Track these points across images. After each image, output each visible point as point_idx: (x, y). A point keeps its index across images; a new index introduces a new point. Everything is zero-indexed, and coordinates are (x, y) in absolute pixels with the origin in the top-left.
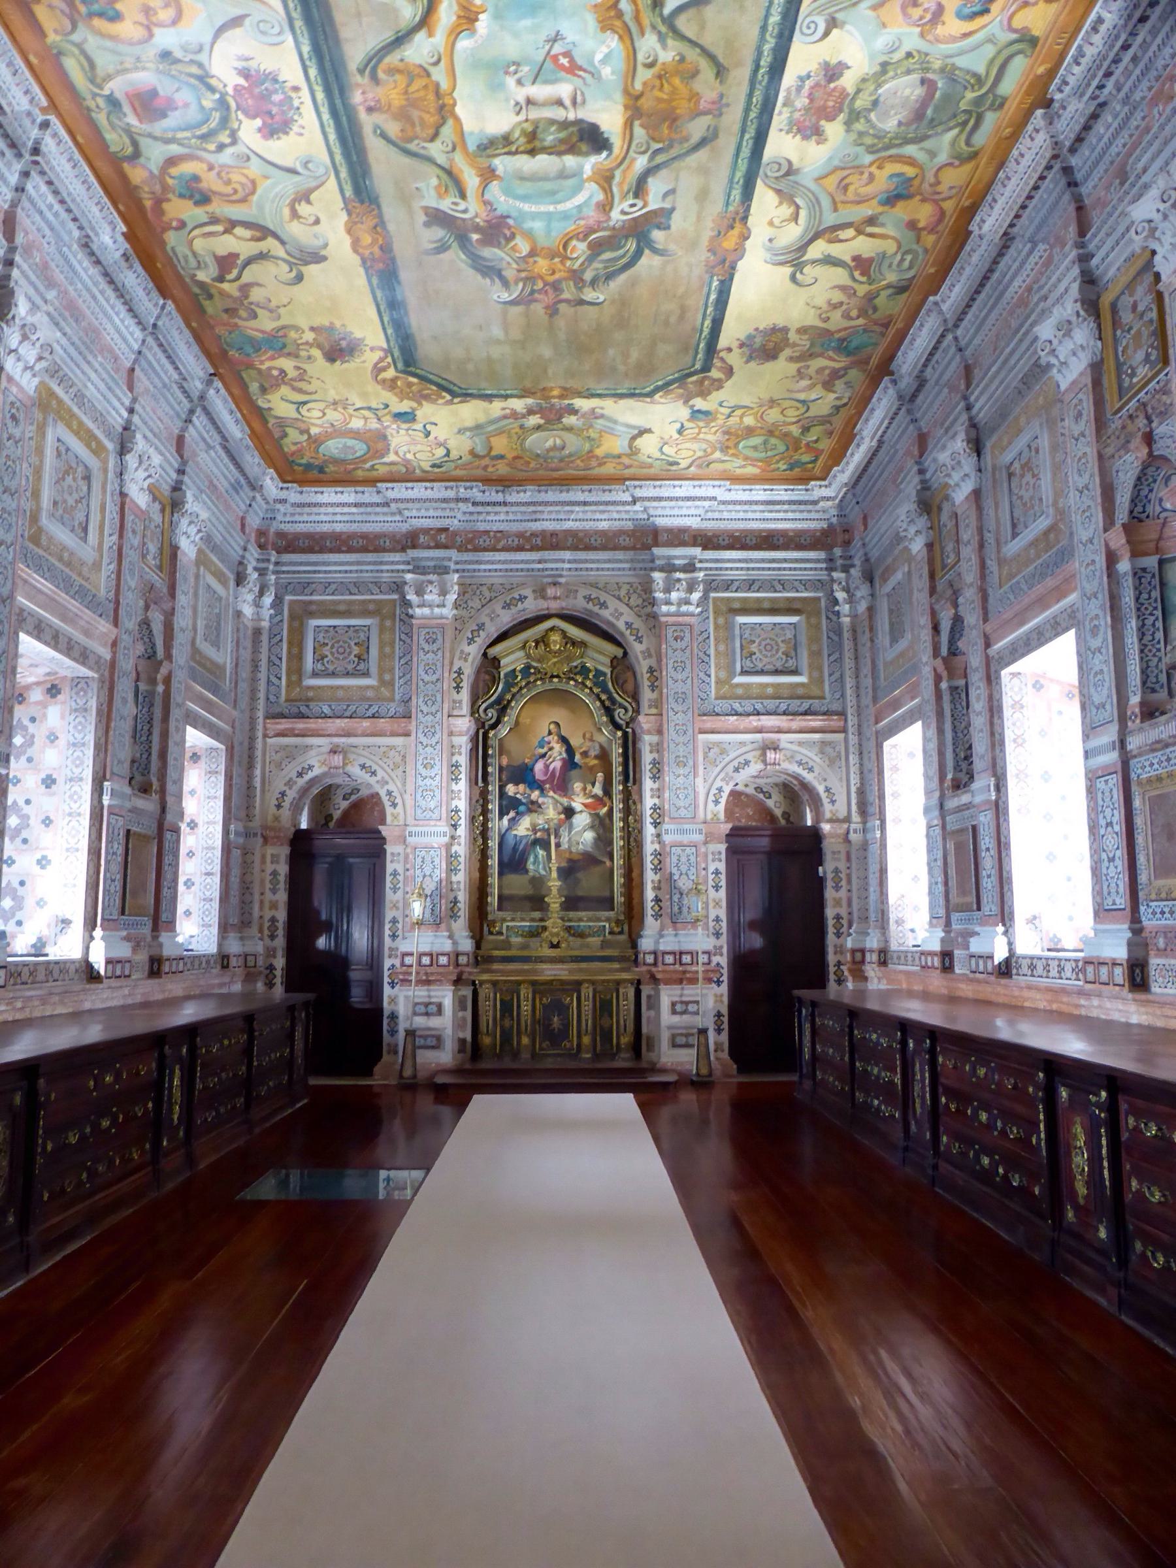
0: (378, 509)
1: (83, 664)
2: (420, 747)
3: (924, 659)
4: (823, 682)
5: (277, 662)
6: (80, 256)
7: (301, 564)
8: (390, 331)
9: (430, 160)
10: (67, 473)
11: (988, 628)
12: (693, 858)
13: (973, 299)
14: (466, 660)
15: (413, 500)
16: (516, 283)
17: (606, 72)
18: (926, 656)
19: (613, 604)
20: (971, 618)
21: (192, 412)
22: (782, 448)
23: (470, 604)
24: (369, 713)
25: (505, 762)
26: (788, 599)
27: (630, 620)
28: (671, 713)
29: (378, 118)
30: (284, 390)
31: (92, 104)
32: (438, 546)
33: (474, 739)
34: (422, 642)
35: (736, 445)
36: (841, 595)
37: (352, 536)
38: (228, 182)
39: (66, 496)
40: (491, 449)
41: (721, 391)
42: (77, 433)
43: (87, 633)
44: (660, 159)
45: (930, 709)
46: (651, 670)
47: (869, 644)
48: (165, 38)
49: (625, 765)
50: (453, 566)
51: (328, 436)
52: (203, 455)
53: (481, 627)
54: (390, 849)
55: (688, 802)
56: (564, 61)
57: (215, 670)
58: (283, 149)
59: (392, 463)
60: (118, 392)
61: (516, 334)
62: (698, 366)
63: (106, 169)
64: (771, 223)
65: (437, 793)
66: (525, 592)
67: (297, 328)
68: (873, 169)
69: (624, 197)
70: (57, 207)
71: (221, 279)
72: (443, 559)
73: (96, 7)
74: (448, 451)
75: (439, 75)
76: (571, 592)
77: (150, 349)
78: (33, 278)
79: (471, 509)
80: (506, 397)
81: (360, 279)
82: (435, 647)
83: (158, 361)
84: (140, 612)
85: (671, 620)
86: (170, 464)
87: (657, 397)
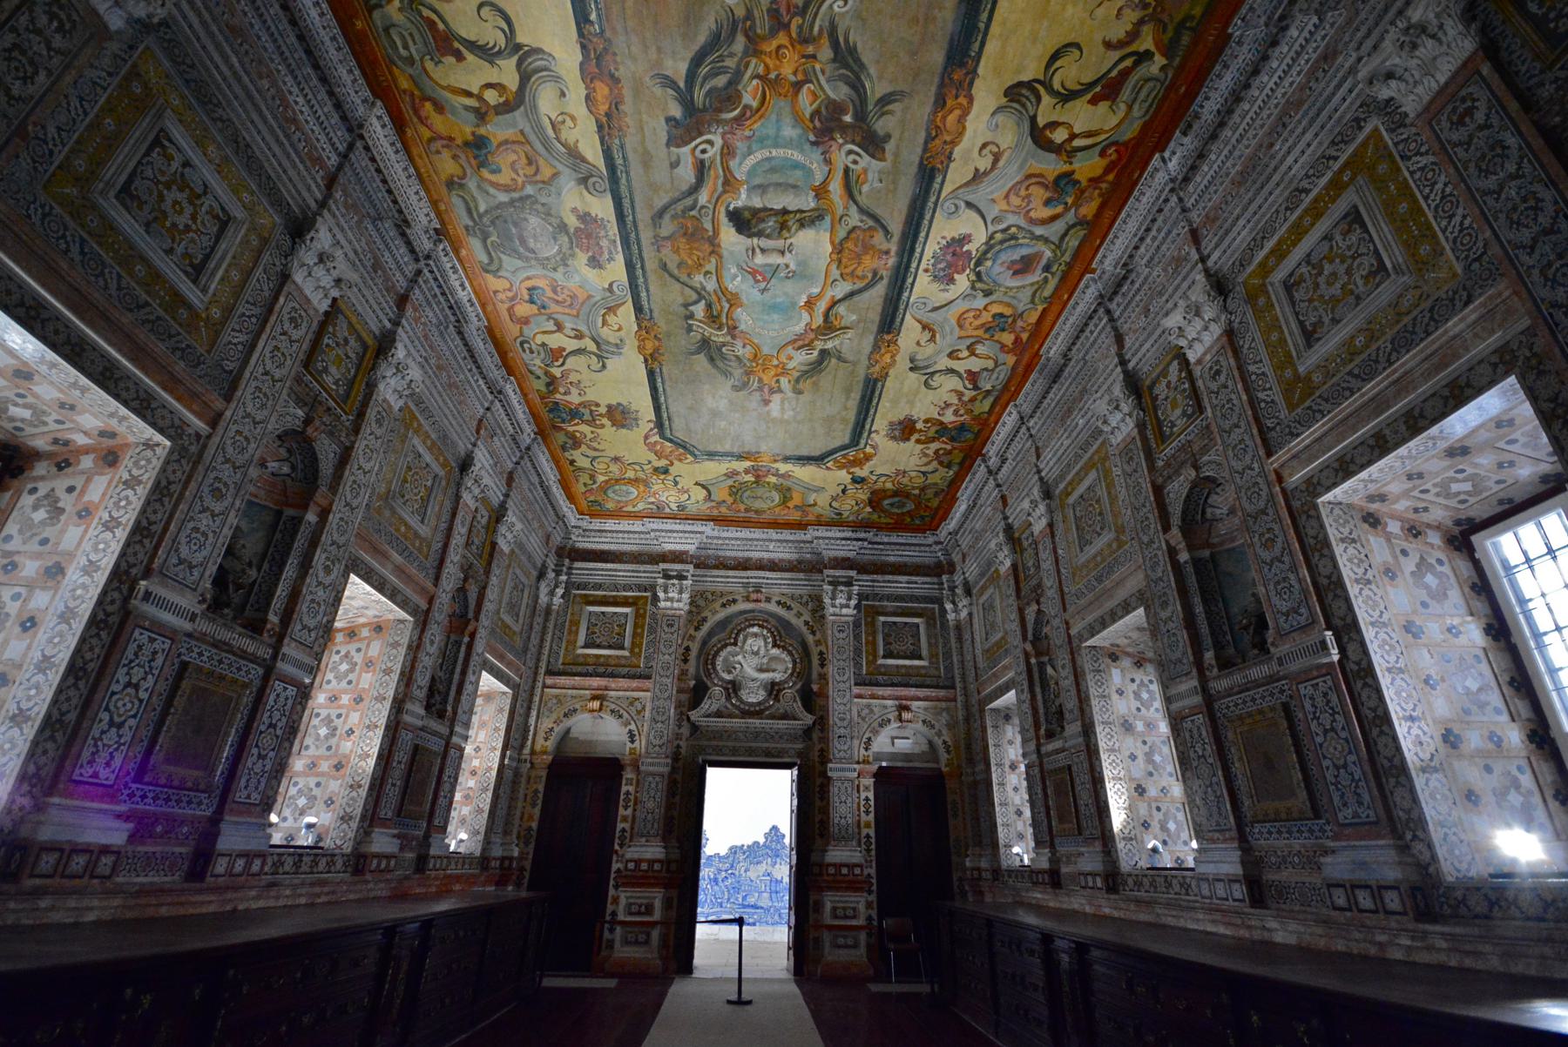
9: (862, 210)
17: (734, 270)
29: (885, 246)
44: (689, 201)
48: (980, 302)
68: (520, 180)
70: (1154, 233)
71: (1145, 56)
75: (835, 273)
81: (992, 47)
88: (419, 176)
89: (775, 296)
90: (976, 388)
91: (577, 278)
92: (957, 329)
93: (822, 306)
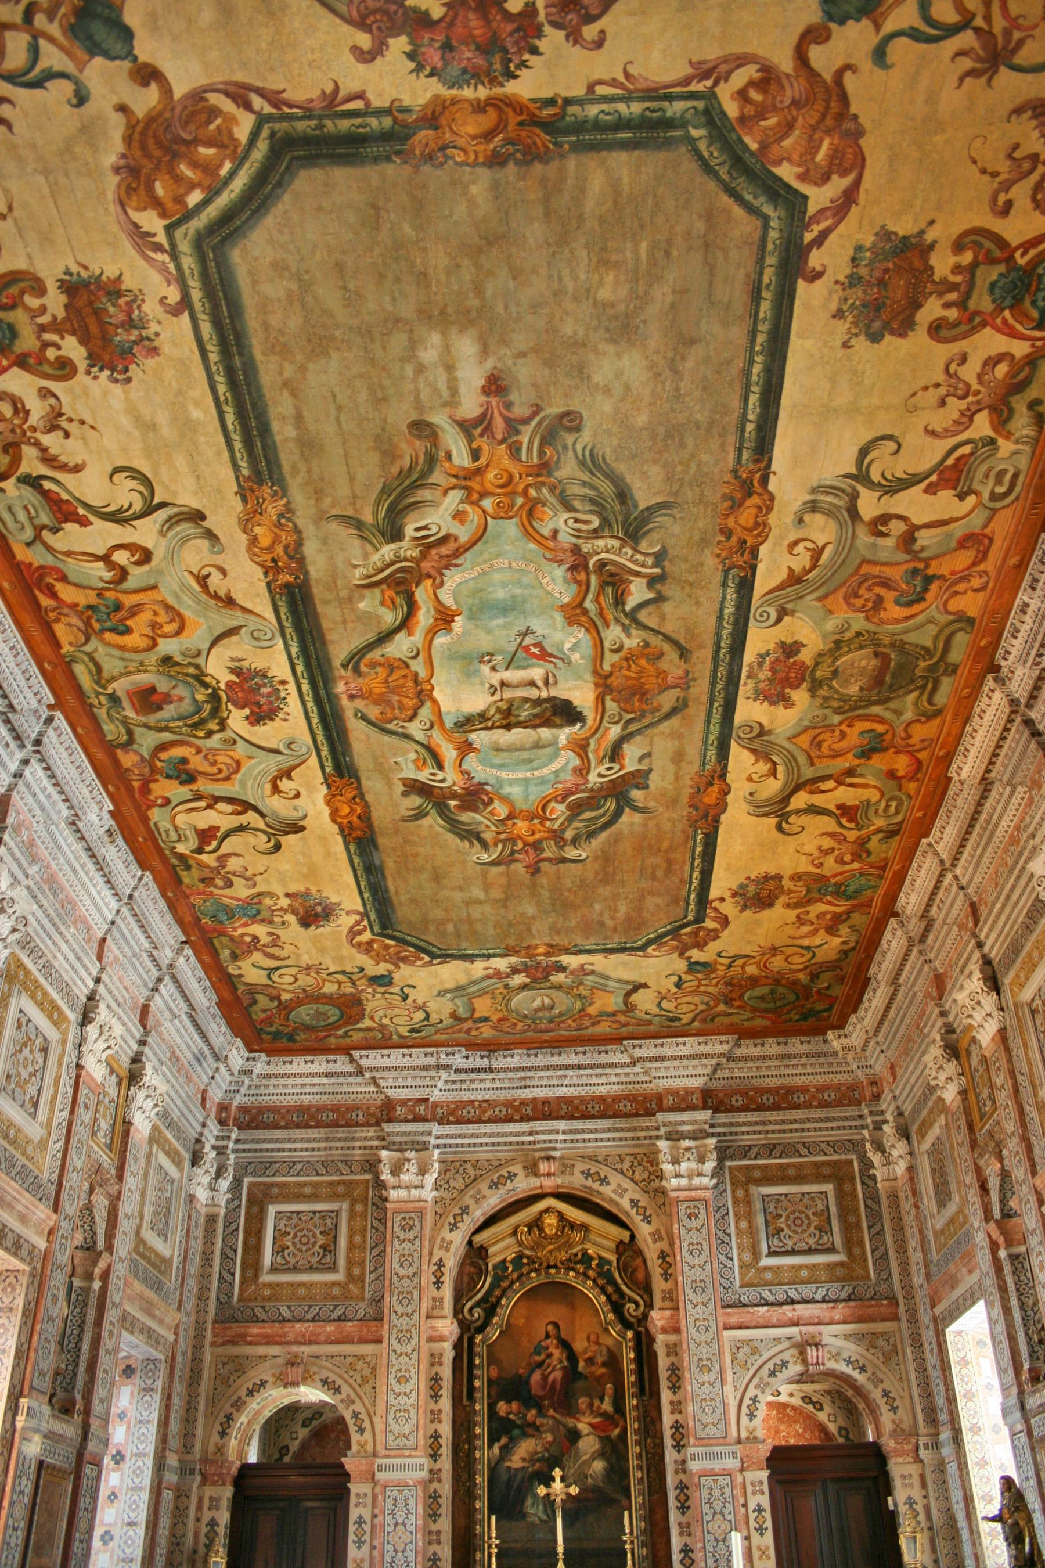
0: (351, 1079)
1: (15, 1255)
2: (393, 1357)
3: (976, 1224)
4: (865, 1260)
5: (231, 1254)
6: (66, 832)
7: (264, 1141)
8: (366, 895)
9: (408, 737)
10: (25, 1045)
11: (1038, 1182)
12: (728, 1491)
13: (965, 840)
14: (447, 1250)
15: (389, 1069)
16: (496, 845)
17: (575, 657)
18: (976, 1221)
19: (615, 1179)
20: (1019, 1173)
21: (160, 980)
22: (792, 997)
23: (453, 1184)
24: (335, 1316)
25: (494, 1372)
26: (815, 1164)
27: (636, 1196)
28: (689, 1307)
29: (359, 704)
30: (257, 956)
31: (96, 702)
32: (418, 1119)
33: (457, 1346)
34: (397, 1229)
35: (741, 997)
36: (876, 1158)
37: (321, 1109)
38: (214, 763)
39: (21, 1069)
40: (473, 1011)
41: (718, 942)
42: (40, 1005)
43: (23, 1219)
44: (633, 727)
45: (990, 1284)
46: (663, 1255)
47: (913, 1211)
48: (168, 647)
49: (639, 1372)
50: (433, 1141)
51: (299, 1002)
52: (167, 1024)
53: (465, 1210)
54: (354, 1488)
55: (717, 1416)
56: (536, 651)
57: (162, 1264)
58: (268, 733)
59: (368, 1029)
60: (86, 962)
61: (496, 893)
62: (690, 917)
63: (100, 755)
64: (750, 779)
65: (413, 1412)
66: (512, 1169)
67: (271, 895)
68: (843, 727)
69: (600, 762)
70: (51, 790)
71: (200, 850)
72: (423, 1133)
73: (109, 624)
74: (428, 1014)
75: (418, 666)
76: (566, 1167)
77: (124, 919)
78: (18, 854)
79: (454, 1076)
80: (489, 956)
82: (412, 1235)
83: (131, 931)
84: (84, 1195)
85: (682, 1195)
86: (132, 1036)
87: (650, 950)
88: (967, 720)
89: (506, 627)
90: (33, 482)
91: (830, 625)
92: (171, 601)
93: (424, 618)
